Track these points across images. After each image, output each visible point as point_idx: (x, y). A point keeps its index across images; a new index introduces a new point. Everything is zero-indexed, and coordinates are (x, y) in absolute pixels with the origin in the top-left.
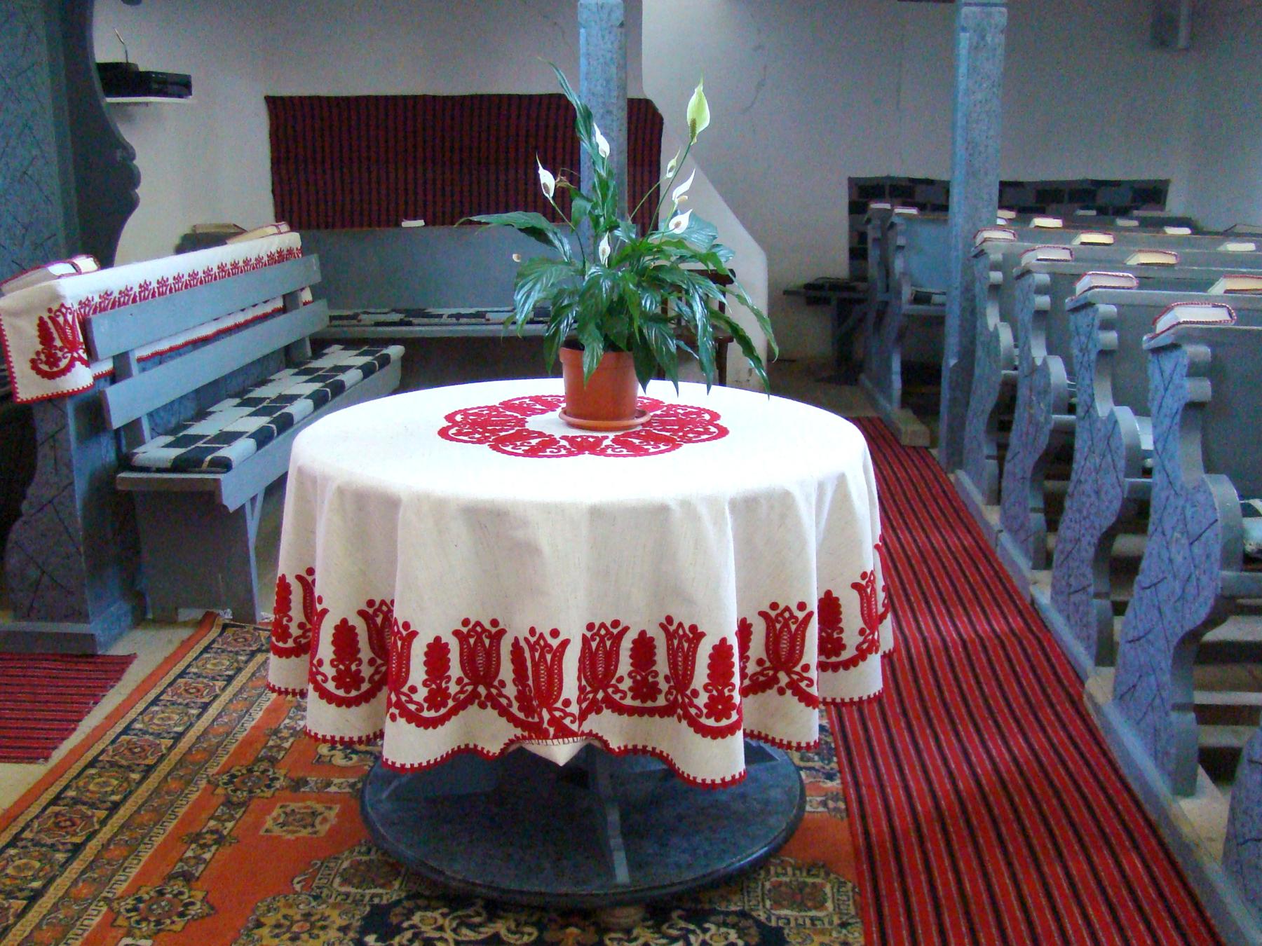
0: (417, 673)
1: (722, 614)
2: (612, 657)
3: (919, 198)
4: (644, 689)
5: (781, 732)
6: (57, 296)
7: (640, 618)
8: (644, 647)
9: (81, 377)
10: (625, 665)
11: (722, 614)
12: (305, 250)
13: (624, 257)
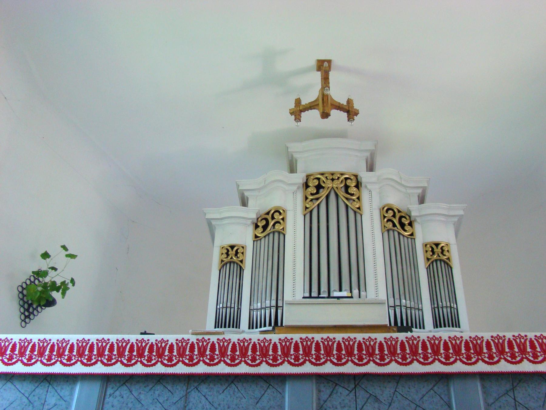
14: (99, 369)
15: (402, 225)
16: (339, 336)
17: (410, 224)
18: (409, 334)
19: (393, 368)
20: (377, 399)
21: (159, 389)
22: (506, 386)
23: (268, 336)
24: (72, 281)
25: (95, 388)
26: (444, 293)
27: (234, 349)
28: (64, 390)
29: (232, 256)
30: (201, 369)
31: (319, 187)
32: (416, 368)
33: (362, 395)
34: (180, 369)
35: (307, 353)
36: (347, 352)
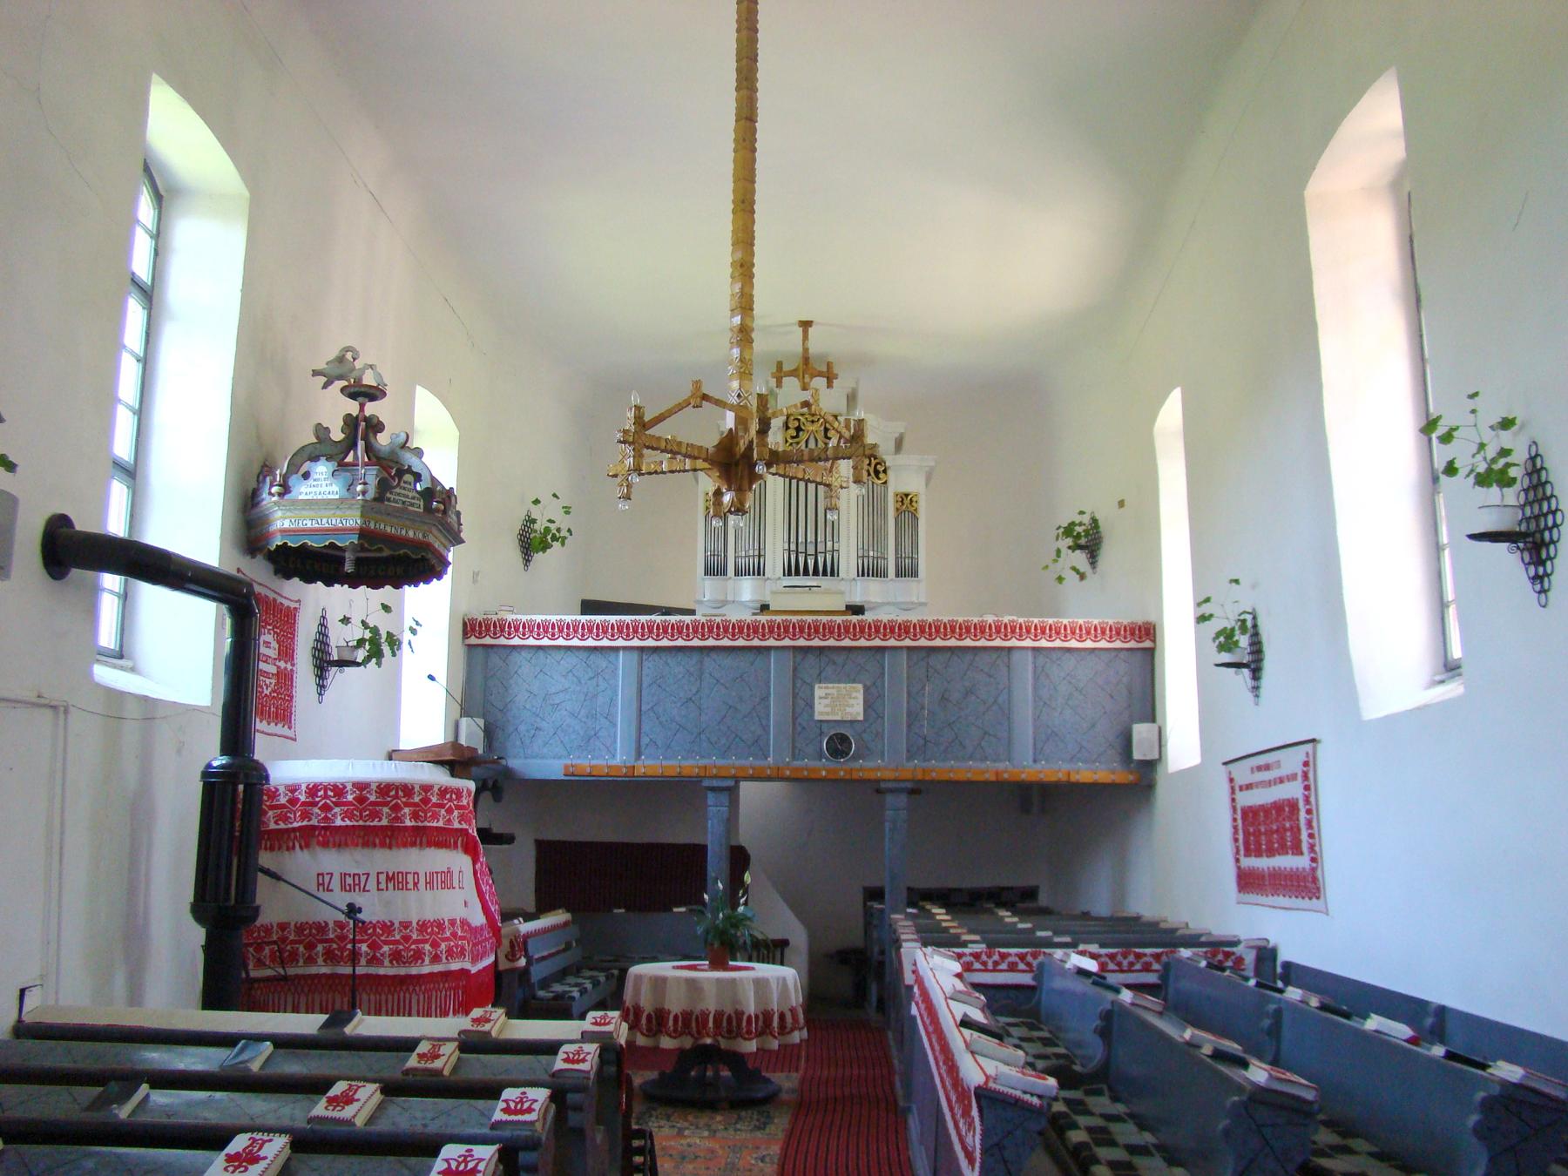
0: (671, 1023)
1: (751, 1008)
4: (730, 1031)
5: (767, 1046)
7: (729, 1010)
8: (730, 1017)
9: (522, 962)
11: (751, 1008)
12: (574, 921)
13: (726, 918)
14: (636, 643)
15: (877, 473)
16: (809, 618)
17: (885, 471)
18: (860, 617)
19: (847, 643)
23: (759, 618)
25: (635, 656)
28: (612, 657)
30: (711, 642)
31: (798, 429)
32: (863, 643)
34: (696, 642)
35: (786, 631)
36: (815, 630)
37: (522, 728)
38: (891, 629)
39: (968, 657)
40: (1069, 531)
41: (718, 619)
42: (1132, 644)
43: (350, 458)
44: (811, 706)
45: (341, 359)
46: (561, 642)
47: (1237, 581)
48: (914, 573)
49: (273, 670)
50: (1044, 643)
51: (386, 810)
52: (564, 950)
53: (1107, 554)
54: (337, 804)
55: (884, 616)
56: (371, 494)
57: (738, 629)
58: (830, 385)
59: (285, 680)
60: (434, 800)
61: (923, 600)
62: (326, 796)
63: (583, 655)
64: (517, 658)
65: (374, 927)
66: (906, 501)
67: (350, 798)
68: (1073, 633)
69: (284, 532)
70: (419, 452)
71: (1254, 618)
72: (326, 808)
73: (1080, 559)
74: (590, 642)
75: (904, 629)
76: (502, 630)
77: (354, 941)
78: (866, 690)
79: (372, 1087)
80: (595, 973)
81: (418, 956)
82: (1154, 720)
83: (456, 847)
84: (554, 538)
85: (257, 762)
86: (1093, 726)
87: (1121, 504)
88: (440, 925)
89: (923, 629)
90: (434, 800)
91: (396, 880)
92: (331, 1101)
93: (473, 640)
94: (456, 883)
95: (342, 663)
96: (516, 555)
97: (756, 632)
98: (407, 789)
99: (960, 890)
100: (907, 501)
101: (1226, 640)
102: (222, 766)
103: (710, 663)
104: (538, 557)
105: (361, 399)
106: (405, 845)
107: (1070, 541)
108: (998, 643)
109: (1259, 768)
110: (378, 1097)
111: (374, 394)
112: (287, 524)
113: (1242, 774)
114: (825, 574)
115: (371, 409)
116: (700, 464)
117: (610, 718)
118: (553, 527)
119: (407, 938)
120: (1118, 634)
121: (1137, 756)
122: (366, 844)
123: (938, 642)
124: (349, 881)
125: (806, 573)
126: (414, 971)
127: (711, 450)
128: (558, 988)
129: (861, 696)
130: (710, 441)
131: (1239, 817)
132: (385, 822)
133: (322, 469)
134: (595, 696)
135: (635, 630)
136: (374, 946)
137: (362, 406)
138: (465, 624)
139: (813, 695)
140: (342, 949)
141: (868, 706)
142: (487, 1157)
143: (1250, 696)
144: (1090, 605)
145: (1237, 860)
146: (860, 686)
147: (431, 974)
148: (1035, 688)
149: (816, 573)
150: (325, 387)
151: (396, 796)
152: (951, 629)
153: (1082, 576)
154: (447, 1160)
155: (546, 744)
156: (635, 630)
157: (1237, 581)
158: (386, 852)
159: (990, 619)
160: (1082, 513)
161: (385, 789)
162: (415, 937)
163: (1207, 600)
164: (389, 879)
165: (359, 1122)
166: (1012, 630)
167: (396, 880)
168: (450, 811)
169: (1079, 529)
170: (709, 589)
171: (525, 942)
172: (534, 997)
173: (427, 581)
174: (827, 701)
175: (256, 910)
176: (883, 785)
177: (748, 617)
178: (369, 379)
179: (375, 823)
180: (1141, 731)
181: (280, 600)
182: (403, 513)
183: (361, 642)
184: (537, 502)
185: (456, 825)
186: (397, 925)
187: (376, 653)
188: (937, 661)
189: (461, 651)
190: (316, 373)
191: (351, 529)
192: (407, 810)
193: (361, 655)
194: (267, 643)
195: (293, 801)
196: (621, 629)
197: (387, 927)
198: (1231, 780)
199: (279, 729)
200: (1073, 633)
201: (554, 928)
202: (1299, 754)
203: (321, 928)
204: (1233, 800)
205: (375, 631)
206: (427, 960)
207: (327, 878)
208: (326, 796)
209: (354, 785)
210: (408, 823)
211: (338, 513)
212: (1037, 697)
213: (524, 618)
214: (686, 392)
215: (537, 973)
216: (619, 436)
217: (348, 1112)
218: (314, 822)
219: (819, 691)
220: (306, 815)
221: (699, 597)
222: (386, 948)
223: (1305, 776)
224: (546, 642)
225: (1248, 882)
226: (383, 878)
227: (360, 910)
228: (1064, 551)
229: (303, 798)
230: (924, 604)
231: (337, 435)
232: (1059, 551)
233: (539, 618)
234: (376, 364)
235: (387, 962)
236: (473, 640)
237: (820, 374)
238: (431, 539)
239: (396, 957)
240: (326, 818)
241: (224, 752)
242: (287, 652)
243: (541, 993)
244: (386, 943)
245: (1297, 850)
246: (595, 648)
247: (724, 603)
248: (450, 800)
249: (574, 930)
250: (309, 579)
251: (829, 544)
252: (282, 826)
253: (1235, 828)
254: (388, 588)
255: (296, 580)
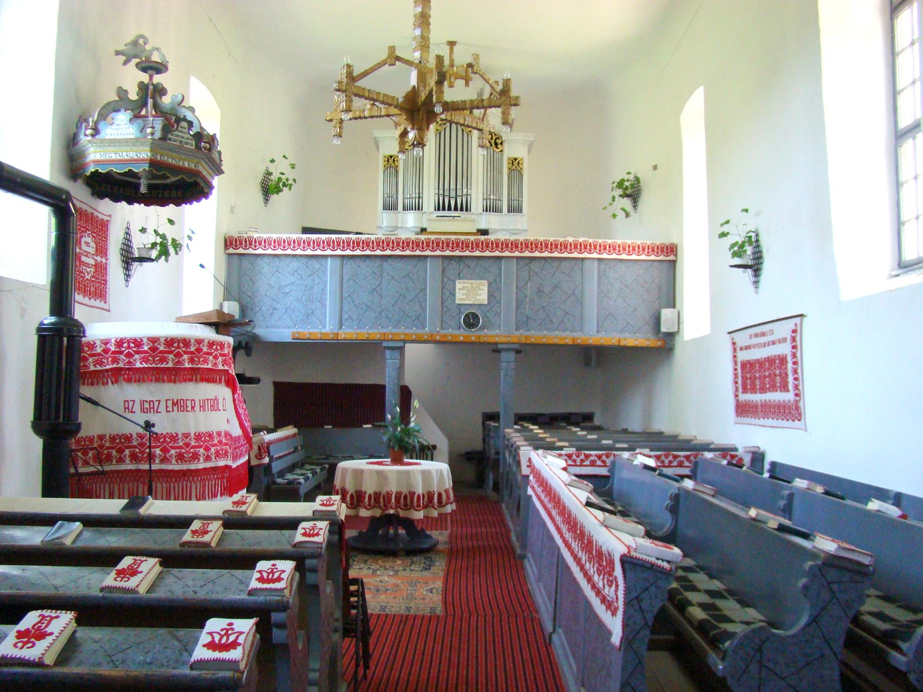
0: (367, 500)
1: (420, 490)
2: (400, 498)
3: (540, 420)
4: (406, 505)
5: (430, 515)
6: (263, 440)
7: (405, 491)
10: (402, 500)
11: (420, 490)
12: (299, 434)
13: (402, 430)
14: (339, 252)
15: (496, 144)
16: (453, 237)
17: (501, 143)
18: (486, 237)
19: (477, 253)
20: (469, 267)
21: (368, 260)
22: (527, 261)
23: (419, 236)
24: (294, 180)
25: (338, 261)
26: (515, 191)
27: (403, 243)
28: (323, 261)
29: (391, 160)
30: (388, 252)
32: (487, 254)
33: (461, 263)
34: (378, 252)
35: (438, 245)
36: (457, 245)
37: (264, 308)
38: (506, 245)
39: (556, 264)
40: (620, 185)
41: (393, 237)
42: (662, 258)
43: (143, 113)
44: (454, 295)
45: (135, 43)
46: (289, 252)
47: (746, 211)
48: (519, 210)
49: (93, 262)
50: (605, 256)
51: (171, 356)
52: (293, 452)
53: (645, 200)
54: (137, 353)
55: (502, 237)
56: (158, 135)
57: (406, 244)
58: (467, 84)
59: (101, 269)
60: (205, 349)
61: (525, 228)
62: (129, 347)
63: (305, 260)
64: (259, 261)
65: (165, 437)
66: (515, 163)
67: (146, 348)
68: (624, 249)
69: (96, 162)
70: (192, 110)
71: (757, 235)
72: (129, 355)
73: (627, 203)
74: (309, 252)
75: (515, 245)
76: (251, 244)
77: (150, 447)
78: (490, 284)
79: (152, 561)
80: (314, 467)
81: (195, 457)
82: (674, 307)
83: (220, 382)
84: (284, 185)
85: (76, 321)
86: (635, 310)
87: (655, 168)
88: (210, 435)
89: (528, 245)
90: (205, 349)
91: (179, 405)
92: (119, 573)
93: (231, 251)
94: (221, 407)
95: (142, 260)
96: (259, 197)
97: (418, 246)
98: (186, 342)
99: (544, 415)
100: (516, 163)
101: (738, 251)
102: (52, 324)
103: (387, 265)
104: (274, 198)
105: (150, 72)
106: (185, 380)
107: (620, 192)
108: (575, 255)
109: (756, 335)
110: (158, 568)
111: (159, 68)
112: (98, 157)
113: (742, 339)
114: (462, 210)
115: (157, 79)
116: (393, 111)
117: (322, 302)
118: (283, 177)
119: (187, 445)
120: (653, 251)
121: (664, 329)
122: (157, 380)
123: (537, 254)
124: (147, 405)
125: (450, 209)
126: (193, 467)
127: (401, 100)
128: (290, 477)
129: (486, 289)
130: (400, 94)
131: (739, 367)
132: (170, 365)
133: (122, 117)
134: (312, 287)
135: (338, 244)
136: (165, 450)
137: (151, 77)
138: (226, 240)
139: (454, 287)
140: (143, 452)
141: (490, 295)
142: (246, 630)
143: (752, 287)
144: (634, 231)
145: (736, 396)
146: (485, 282)
147: (205, 469)
148: (599, 286)
149: (456, 209)
150: (125, 63)
151: (178, 347)
152: (546, 245)
153: (627, 215)
154: (210, 634)
155: (279, 319)
156: (338, 244)
157: (746, 211)
158: (171, 385)
159: (571, 239)
160: (629, 173)
161: (170, 342)
162: (193, 443)
163: (727, 222)
164: (174, 404)
165: (142, 590)
166: (584, 247)
167: (179, 405)
168: (216, 357)
169: (626, 184)
170: (386, 219)
171: (268, 448)
172: (274, 483)
173: (198, 200)
174: (464, 292)
175: (79, 425)
176: (500, 346)
177: (413, 237)
178: (156, 57)
179: (164, 365)
180: (667, 314)
181: (96, 214)
182: (180, 149)
183: (154, 245)
184: (272, 161)
185: (220, 367)
186: (180, 436)
187: (164, 252)
188: (535, 266)
189: (223, 259)
190: (118, 53)
191: (143, 160)
192: (186, 357)
193: (154, 254)
194: (86, 244)
195: (106, 351)
196: (329, 243)
197: (174, 438)
198: (734, 344)
199: (98, 303)
200: (624, 249)
201: (287, 438)
202: (790, 324)
203: (128, 438)
204: (735, 357)
205: (163, 237)
206: (202, 459)
207: (131, 404)
208: (129, 347)
209: (149, 339)
210: (187, 365)
211: (134, 148)
212: (600, 291)
213: (265, 236)
214: (384, 56)
215: (276, 467)
216: (335, 86)
217: (132, 582)
218: (121, 365)
219: (459, 285)
220: (115, 360)
221: (379, 224)
222: (173, 452)
223: (794, 339)
224: (279, 252)
225: (743, 409)
226: (170, 404)
227: (153, 426)
228: (617, 198)
229: (113, 349)
230: (526, 230)
231: (133, 96)
232: (614, 198)
233: (274, 236)
234: (162, 46)
235: (174, 461)
236: (231, 251)
237: (461, 78)
238: (201, 168)
239: (180, 458)
240: (129, 362)
241: (52, 313)
242: (102, 250)
243: (279, 480)
244: (173, 448)
245: (784, 388)
246: (312, 256)
247: (396, 228)
248: (216, 350)
249: (299, 440)
250: (116, 199)
251: (465, 190)
252: (99, 368)
253: (736, 375)
254: (172, 206)
255: (107, 200)
